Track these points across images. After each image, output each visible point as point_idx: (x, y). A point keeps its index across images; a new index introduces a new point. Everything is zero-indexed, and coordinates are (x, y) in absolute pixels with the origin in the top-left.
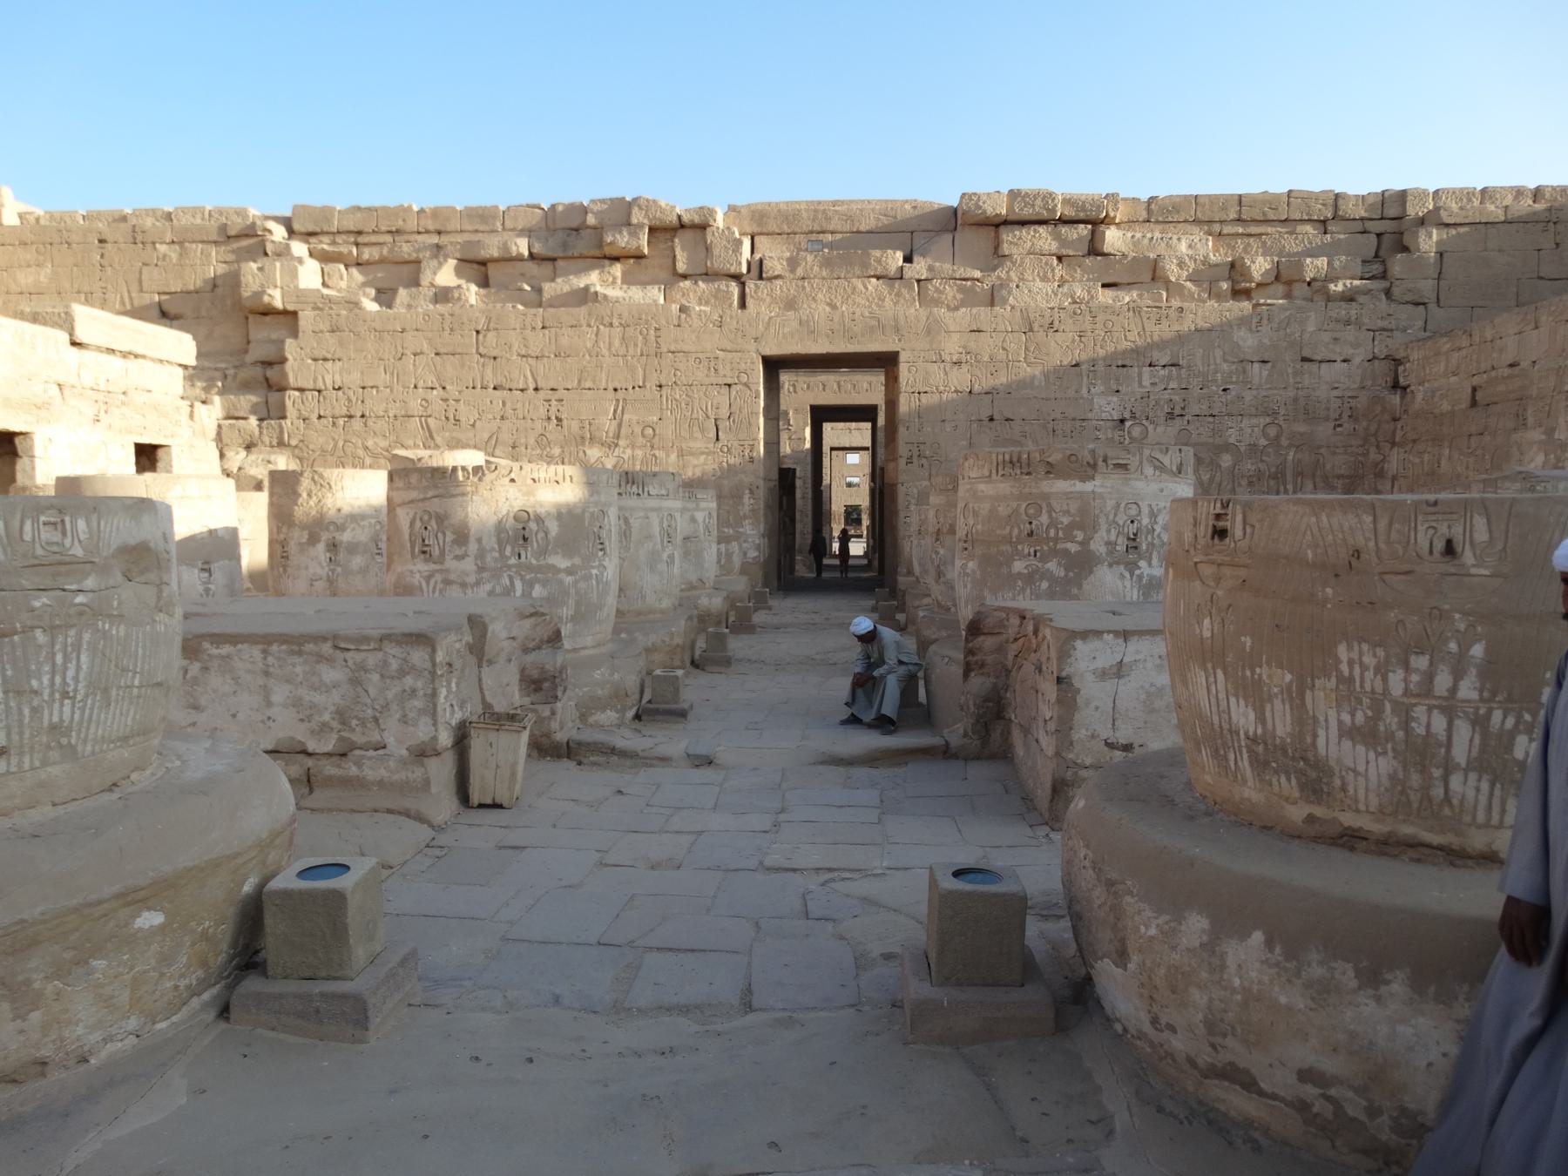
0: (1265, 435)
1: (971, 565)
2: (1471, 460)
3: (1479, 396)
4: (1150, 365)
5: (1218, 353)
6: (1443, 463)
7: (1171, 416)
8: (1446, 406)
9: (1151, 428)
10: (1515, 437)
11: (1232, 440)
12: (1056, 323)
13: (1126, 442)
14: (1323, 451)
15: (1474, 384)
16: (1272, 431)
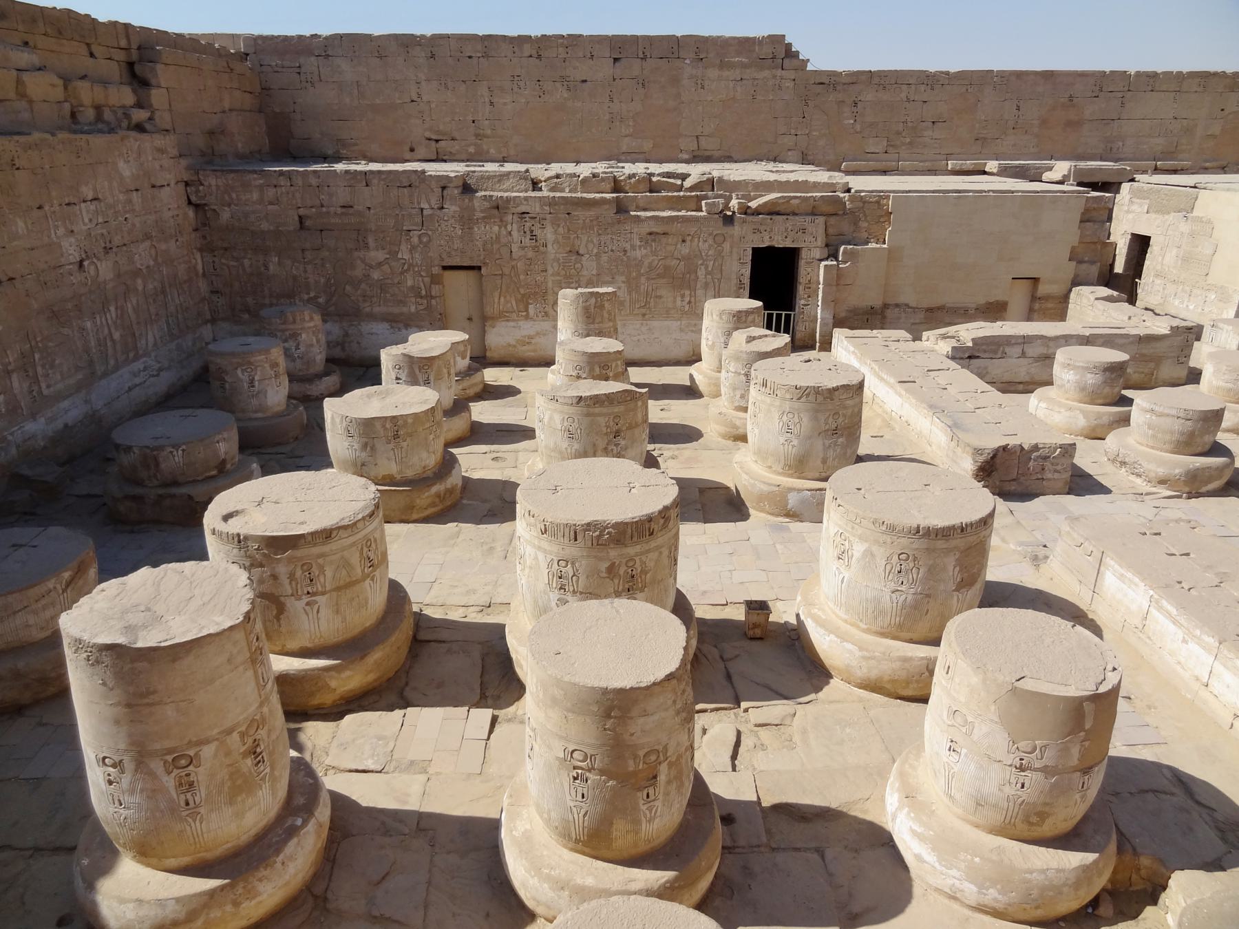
0: (151, 256)
1: (840, 440)
2: (309, 268)
3: (308, 223)
4: (84, 201)
5: (115, 184)
6: (271, 267)
7: (107, 250)
8: (265, 226)
9: (99, 265)
10: (361, 254)
11: (139, 266)
12: (17, 162)
13: (89, 283)
14: (175, 263)
15: (301, 213)
16: (153, 252)
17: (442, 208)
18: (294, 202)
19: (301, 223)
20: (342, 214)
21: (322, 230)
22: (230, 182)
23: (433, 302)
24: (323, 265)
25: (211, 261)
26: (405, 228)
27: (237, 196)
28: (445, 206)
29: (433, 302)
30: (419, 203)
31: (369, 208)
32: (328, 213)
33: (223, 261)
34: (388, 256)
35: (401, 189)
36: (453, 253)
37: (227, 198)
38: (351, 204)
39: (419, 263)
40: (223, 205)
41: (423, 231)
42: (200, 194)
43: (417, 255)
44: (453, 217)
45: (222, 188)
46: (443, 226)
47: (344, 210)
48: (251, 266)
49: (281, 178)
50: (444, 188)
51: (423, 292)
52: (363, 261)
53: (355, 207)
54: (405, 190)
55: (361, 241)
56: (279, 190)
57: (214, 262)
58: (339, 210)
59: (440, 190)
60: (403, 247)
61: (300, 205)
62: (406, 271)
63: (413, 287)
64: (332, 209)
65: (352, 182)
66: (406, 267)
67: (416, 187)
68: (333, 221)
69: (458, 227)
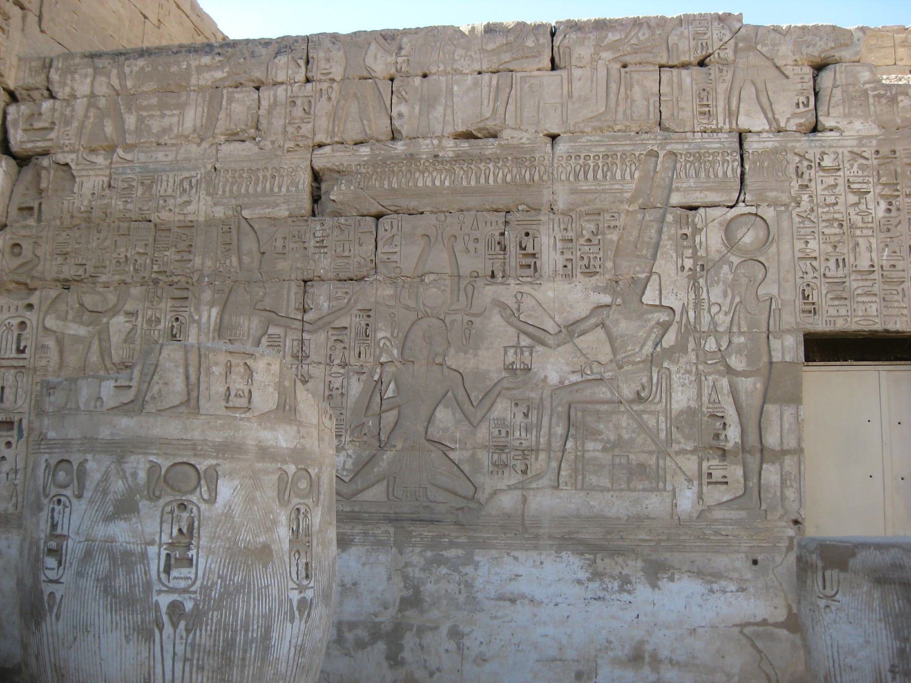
3: (336, 193)
10: (507, 292)
15: (318, 165)
17: (815, 130)
18: (306, 129)
19: (316, 199)
20: (459, 158)
21: (378, 217)
22: (129, 84)
23: (771, 474)
24: (366, 334)
25: (15, 322)
26: (676, 199)
27: (141, 120)
28: (827, 122)
29: (771, 474)
30: (733, 114)
31: (554, 137)
32: (412, 157)
33: (51, 322)
34: (606, 299)
35: (666, 75)
36: (854, 284)
37: (109, 128)
38: (490, 124)
39: (723, 320)
40: (93, 151)
41: (741, 209)
42: (38, 125)
43: (716, 294)
44: (856, 155)
45: (102, 103)
46: (818, 188)
47: (465, 145)
48: (129, 338)
49: (282, 60)
50: (819, 68)
51: (733, 434)
52: (512, 315)
53: (506, 134)
54: (684, 72)
55: (513, 248)
56: (265, 94)
57: (23, 324)
58: (450, 147)
59: (808, 71)
60: (666, 266)
61: (321, 138)
62: (669, 353)
63: (691, 413)
64: (425, 147)
65: (506, 57)
66: (670, 339)
67: (725, 63)
68: (423, 181)
69: (875, 190)
